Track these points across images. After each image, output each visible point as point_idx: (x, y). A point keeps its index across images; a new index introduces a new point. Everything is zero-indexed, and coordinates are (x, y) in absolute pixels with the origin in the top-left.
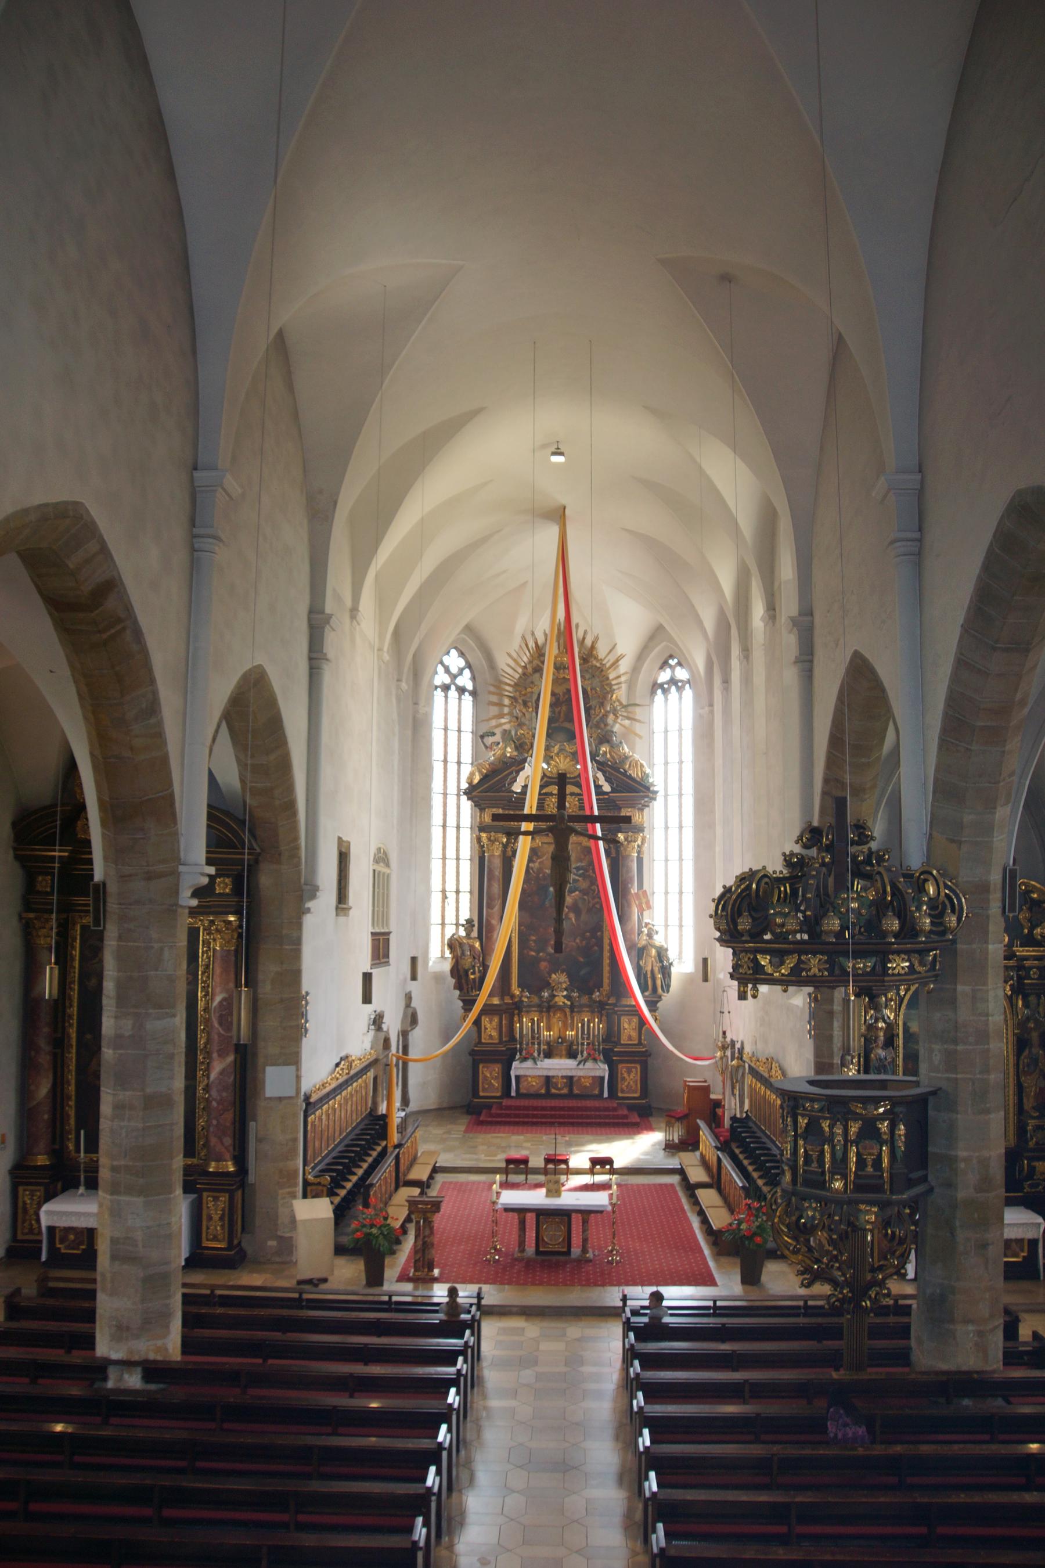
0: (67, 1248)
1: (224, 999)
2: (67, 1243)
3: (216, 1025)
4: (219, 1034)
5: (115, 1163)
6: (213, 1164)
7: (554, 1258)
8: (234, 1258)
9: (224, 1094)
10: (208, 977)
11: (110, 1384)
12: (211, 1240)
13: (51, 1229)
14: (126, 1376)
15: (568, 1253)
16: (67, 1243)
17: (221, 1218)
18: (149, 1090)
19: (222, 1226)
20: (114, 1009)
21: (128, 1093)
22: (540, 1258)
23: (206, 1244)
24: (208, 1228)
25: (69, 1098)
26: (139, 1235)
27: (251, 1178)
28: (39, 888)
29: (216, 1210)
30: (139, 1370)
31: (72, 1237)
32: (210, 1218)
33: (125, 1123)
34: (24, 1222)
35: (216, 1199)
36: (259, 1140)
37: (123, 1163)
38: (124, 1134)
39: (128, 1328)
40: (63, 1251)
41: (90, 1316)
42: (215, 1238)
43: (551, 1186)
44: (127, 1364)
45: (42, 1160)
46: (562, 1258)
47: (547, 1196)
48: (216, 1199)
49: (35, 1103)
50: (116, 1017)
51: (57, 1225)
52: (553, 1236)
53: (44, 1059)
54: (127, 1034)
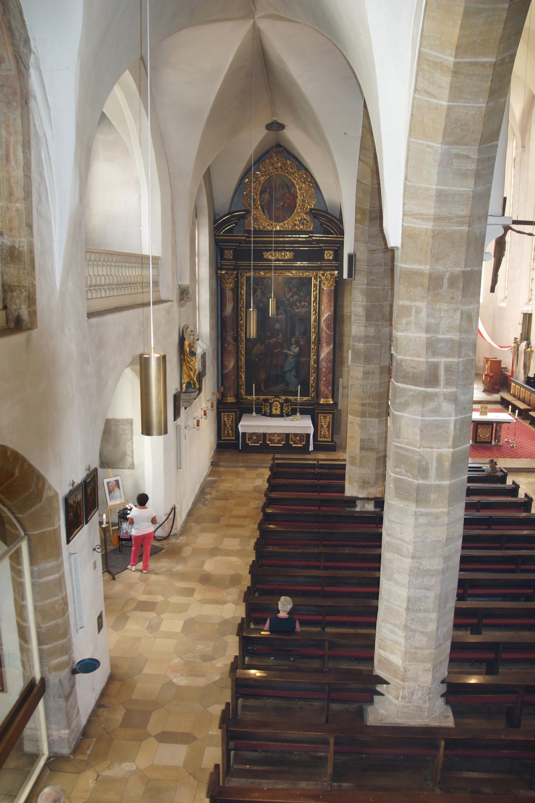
0: (251, 443)
1: (329, 315)
2: (252, 441)
3: (325, 328)
4: (326, 333)
5: (364, 402)
6: (322, 400)
7: (485, 445)
8: (331, 447)
9: (329, 365)
10: (316, 304)
11: (358, 509)
12: (226, 437)
13: (244, 434)
14: (366, 505)
15: (491, 442)
16: (252, 441)
17: (328, 427)
18: (382, 364)
19: (328, 431)
20: (364, 322)
21: (371, 366)
22: (478, 445)
23: (319, 439)
24: (321, 432)
25: (241, 368)
26: (375, 438)
27: (340, 407)
28: (226, 257)
29: (325, 423)
30: (373, 502)
31: (255, 438)
32: (322, 427)
33: (370, 381)
34: (224, 431)
35: (325, 417)
36: (344, 388)
37: (368, 401)
38: (369, 387)
39: (368, 483)
40: (250, 444)
41: (342, 477)
42: (324, 436)
43: (483, 410)
44: (367, 499)
45: (231, 400)
46: (489, 445)
47: (480, 415)
48: (325, 417)
49: (228, 371)
50: (365, 326)
51: (247, 432)
52: (484, 434)
53: (231, 348)
54: (371, 335)
